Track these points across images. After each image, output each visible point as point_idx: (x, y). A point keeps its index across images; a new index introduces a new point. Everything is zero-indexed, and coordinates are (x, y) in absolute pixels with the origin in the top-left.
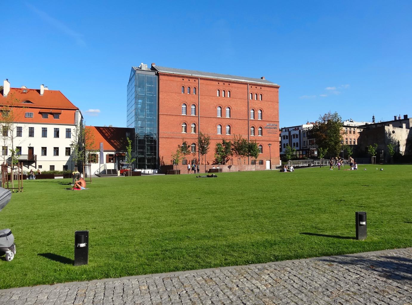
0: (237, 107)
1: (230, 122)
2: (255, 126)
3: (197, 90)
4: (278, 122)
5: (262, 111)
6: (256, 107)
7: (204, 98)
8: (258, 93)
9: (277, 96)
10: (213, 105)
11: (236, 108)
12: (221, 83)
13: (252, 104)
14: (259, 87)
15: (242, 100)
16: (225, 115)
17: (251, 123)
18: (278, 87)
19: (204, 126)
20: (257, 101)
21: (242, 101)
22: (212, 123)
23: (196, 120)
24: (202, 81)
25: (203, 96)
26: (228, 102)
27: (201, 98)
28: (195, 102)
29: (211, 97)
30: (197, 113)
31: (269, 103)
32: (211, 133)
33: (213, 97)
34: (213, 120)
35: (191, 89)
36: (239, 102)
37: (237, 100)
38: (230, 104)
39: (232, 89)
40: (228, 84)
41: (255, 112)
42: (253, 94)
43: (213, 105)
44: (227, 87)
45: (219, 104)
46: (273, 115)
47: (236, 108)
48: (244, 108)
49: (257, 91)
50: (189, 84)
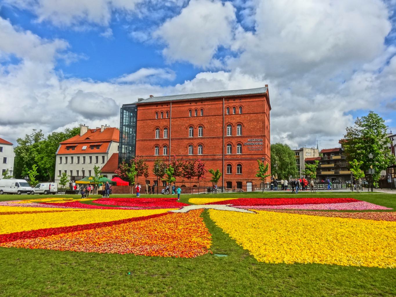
2: (232, 143)
6: (234, 121)
8: (237, 106)
11: (210, 126)
13: (229, 119)
16: (197, 135)
20: (235, 116)
26: (200, 120)
29: (183, 118)
31: (252, 115)
33: (185, 118)
37: (211, 117)
38: (202, 123)
41: (233, 128)
46: (258, 129)
49: (235, 105)
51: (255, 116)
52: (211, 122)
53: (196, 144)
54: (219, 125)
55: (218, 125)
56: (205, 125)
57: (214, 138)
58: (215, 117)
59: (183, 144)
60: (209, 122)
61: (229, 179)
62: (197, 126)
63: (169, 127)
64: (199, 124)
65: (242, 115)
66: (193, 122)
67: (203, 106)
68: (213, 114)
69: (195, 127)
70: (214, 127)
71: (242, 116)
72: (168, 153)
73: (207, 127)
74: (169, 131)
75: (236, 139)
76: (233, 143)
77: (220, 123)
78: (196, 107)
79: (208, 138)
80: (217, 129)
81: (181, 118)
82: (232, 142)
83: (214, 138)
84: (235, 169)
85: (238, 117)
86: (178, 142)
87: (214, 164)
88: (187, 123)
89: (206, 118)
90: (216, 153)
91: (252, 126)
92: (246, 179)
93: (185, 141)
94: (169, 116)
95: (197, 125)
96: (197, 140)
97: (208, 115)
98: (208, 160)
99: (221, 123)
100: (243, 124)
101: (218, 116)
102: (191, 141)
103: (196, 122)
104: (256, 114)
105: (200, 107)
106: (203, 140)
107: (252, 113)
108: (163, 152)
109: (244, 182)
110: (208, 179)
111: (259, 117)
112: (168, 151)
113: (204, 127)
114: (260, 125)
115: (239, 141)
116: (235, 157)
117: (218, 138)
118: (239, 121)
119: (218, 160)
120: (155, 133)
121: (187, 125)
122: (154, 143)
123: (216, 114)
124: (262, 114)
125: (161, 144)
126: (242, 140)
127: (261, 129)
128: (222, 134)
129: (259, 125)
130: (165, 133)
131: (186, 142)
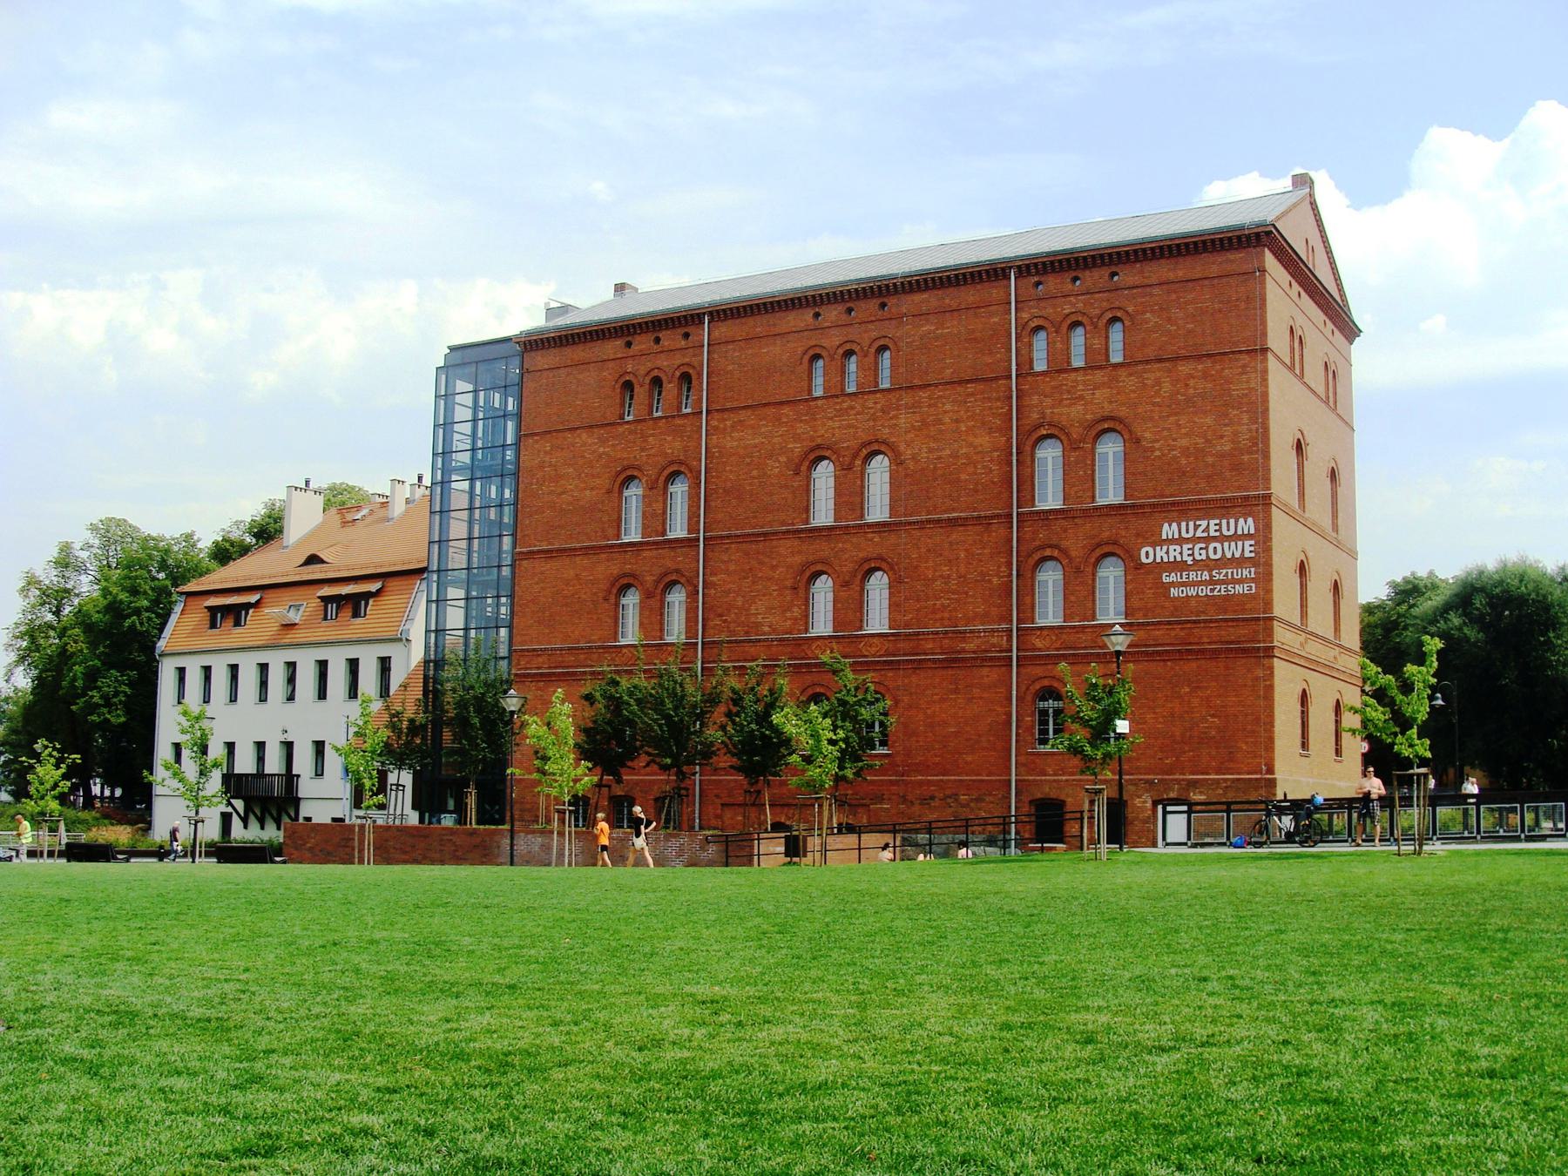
0: (935, 440)
2: (1064, 552)
6: (1073, 414)
10: (783, 459)
11: (931, 450)
14: (1094, 278)
15: (971, 387)
17: (1035, 532)
19: (728, 592)
21: (972, 394)
32: (766, 629)
36: (948, 407)
40: (873, 304)
44: (871, 326)
45: (819, 441)
46: (1222, 456)
47: (931, 450)
51: (1206, 375)
52: (939, 422)
53: (850, 566)
54: (983, 440)
56: (902, 447)
59: (774, 568)
60: (925, 424)
61: (1050, 784)
62: (855, 456)
64: (865, 438)
65: (1123, 373)
66: (830, 428)
70: (955, 456)
71: (1128, 381)
73: (913, 458)
76: (1073, 554)
77: (990, 431)
80: (975, 465)
82: (1064, 544)
86: (747, 554)
87: (956, 691)
88: (797, 438)
90: (968, 621)
92: (1151, 782)
93: (784, 547)
95: (854, 444)
97: (917, 382)
98: (919, 666)
99: (999, 430)
101: (981, 386)
102: (823, 549)
103: (850, 426)
104: (1209, 363)
105: (875, 334)
107: (1183, 352)
109: (1137, 801)
110: (921, 783)
111: (1228, 382)
114: (1235, 434)
115: (1106, 535)
116: (1085, 638)
117: (983, 522)
119: (981, 660)
129: (1228, 431)
131: (790, 555)
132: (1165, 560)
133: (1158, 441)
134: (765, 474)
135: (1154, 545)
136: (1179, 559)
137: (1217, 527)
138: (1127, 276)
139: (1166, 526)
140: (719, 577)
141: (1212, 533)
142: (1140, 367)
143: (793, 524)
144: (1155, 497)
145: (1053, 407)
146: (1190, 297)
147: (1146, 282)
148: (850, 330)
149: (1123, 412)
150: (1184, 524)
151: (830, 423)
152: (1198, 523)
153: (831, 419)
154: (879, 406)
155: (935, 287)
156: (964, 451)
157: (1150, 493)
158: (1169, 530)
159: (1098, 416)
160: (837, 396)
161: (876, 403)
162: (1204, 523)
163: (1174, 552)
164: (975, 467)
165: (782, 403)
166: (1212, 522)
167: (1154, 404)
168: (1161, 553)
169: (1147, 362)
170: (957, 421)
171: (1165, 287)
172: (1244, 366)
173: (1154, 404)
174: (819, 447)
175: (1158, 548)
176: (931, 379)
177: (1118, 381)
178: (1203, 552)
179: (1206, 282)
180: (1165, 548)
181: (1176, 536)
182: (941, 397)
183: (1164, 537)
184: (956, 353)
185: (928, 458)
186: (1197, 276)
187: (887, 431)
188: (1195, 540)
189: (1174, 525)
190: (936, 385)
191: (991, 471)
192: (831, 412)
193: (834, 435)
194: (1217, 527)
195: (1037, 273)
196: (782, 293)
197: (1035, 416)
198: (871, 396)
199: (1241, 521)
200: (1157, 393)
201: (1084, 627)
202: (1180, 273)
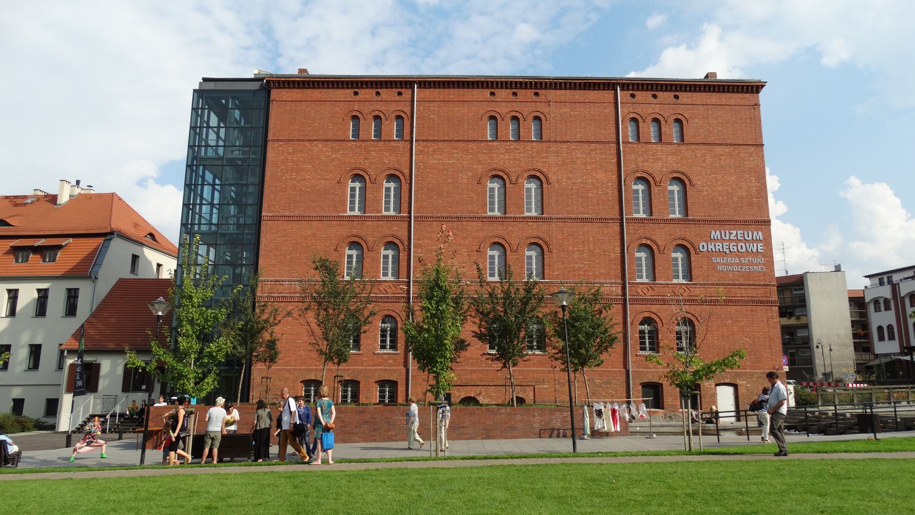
1: (540, 230)
3: (407, 123)
4: (765, 222)
5: (687, 182)
7: (434, 151)
8: (666, 114)
9: (756, 121)
10: (470, 174)
11: (569, 178)
12: (502, 94)
14: (665, 96)
16: (520, 207)
18: (754, 88)
20: (659, 147)
21: (594, 150)
22: (464, 238)
23: (400, 231)
24: (428, 93)
25: (429, 144)
27: (418, 151)
28: (396, 166)
29: (461, 145)
30: (405, 206)
31: (718, 149)
33: (471, 145)
34: (470, 228)
35: (385, 124)
36: (579, 155)
37: (573, 146)
38: (539, 166)
39: (546, 110)
40: (530, 93)
41: (655, 190)
42: (640, 121)
43: (470, 174)
45: (495, 166)
46: (742, 198)
47: (569, 178)
48: (601, 176)
49: (657, 110)
50: (379, 107)
55: (598, 176)
56: (550, 175)
57: (586, 220)
58: (586, 146)
63: (406, 172)
66: (503, 158)
67: (542, 107)
68: (578, 137)
69: (514, 180)
72: (403, 270)
74: (405, 187)
75: (668, 228)
76: (659, 243)
78: (517, 107)
79: (564, 220)
81: (456, 144)
82: (653, 237)
83: (586, 220)
84: (666, 338)
85: (672, 154)
89: (553, 147)
91: (720, 188)
94: (407, 130)
96: (520, 225)
97: (558, 139)
100: (691, 177)
101: (599, 146)
104: (732, 148)
106: (545, 226)
107: (717, 142)
108: (378, 267)
112: (403, 264)
113: (547, 180)
115: (678, 234)
118: (676, 167)
120: (345, 192)
121: (480, 169)
122: (345, 230)
123: (592, 139)
124: (752, 149)
125: (371, 233)
126: (688, 233)
127: (755, 200)
128: (617, 208)
130: (388, 196)
132: (714, 250)
133: (705, 187)
134: (457, 181)
135: (706, 242)
136: (721, 250)
137: (742, 235)
138: (685, 97)
139: (713, 232)
140: (424, 242)
141: (739, 238)
142: (693, 146)
143: (477, 213)
144: (705, 216)
145: (643, 162)
146: (720, 114)
147: (694, 102)
148: (514, 104)
149: (684, 169)
150: (723, 232)
151: (502, 156)
152: (731, 232)
153: (503, 154)
154: (535, 150)
155: (570, 89)
156: (590, 181)
157: (702, 214)
158: (716, 234)
159: (670, 170)
160: (506, 141)
161: (533, 148)
162: (734, 232)
163: (719, 246)
164: (597, 190)
165: (470, 141)
166: (739, 232)
167: (702, 167)
168: (711, 247)
169: (697, 144)
170: (585, 164)
171: (705, 106)
172: (751, 153)
173: (702, 167)
174: (495, 169)
175: (709, 244)
176: (568, 138)
177: (681, 153)
178: (735, 248)
179: (728, 107)
180: (713, 244)
181: (719, 238)
182: (574, 149)
183: (712, 238)
184: (583, 125)
185: (567, 182)
186: (722, 103)
187: (540, 164)
188: (730, 240)
189: (718, 233)
190: (571, 142)
191: (607, 193)
192: (502, 150)
193: (504, 164)
194: (742, 235)
195: (633, 90)
196: (473, 77)
197: (633, 166)
198: (529, 144)
199: (755, 233)
200: (704, 161)
201: (668, 284)
202: (713, 101)
